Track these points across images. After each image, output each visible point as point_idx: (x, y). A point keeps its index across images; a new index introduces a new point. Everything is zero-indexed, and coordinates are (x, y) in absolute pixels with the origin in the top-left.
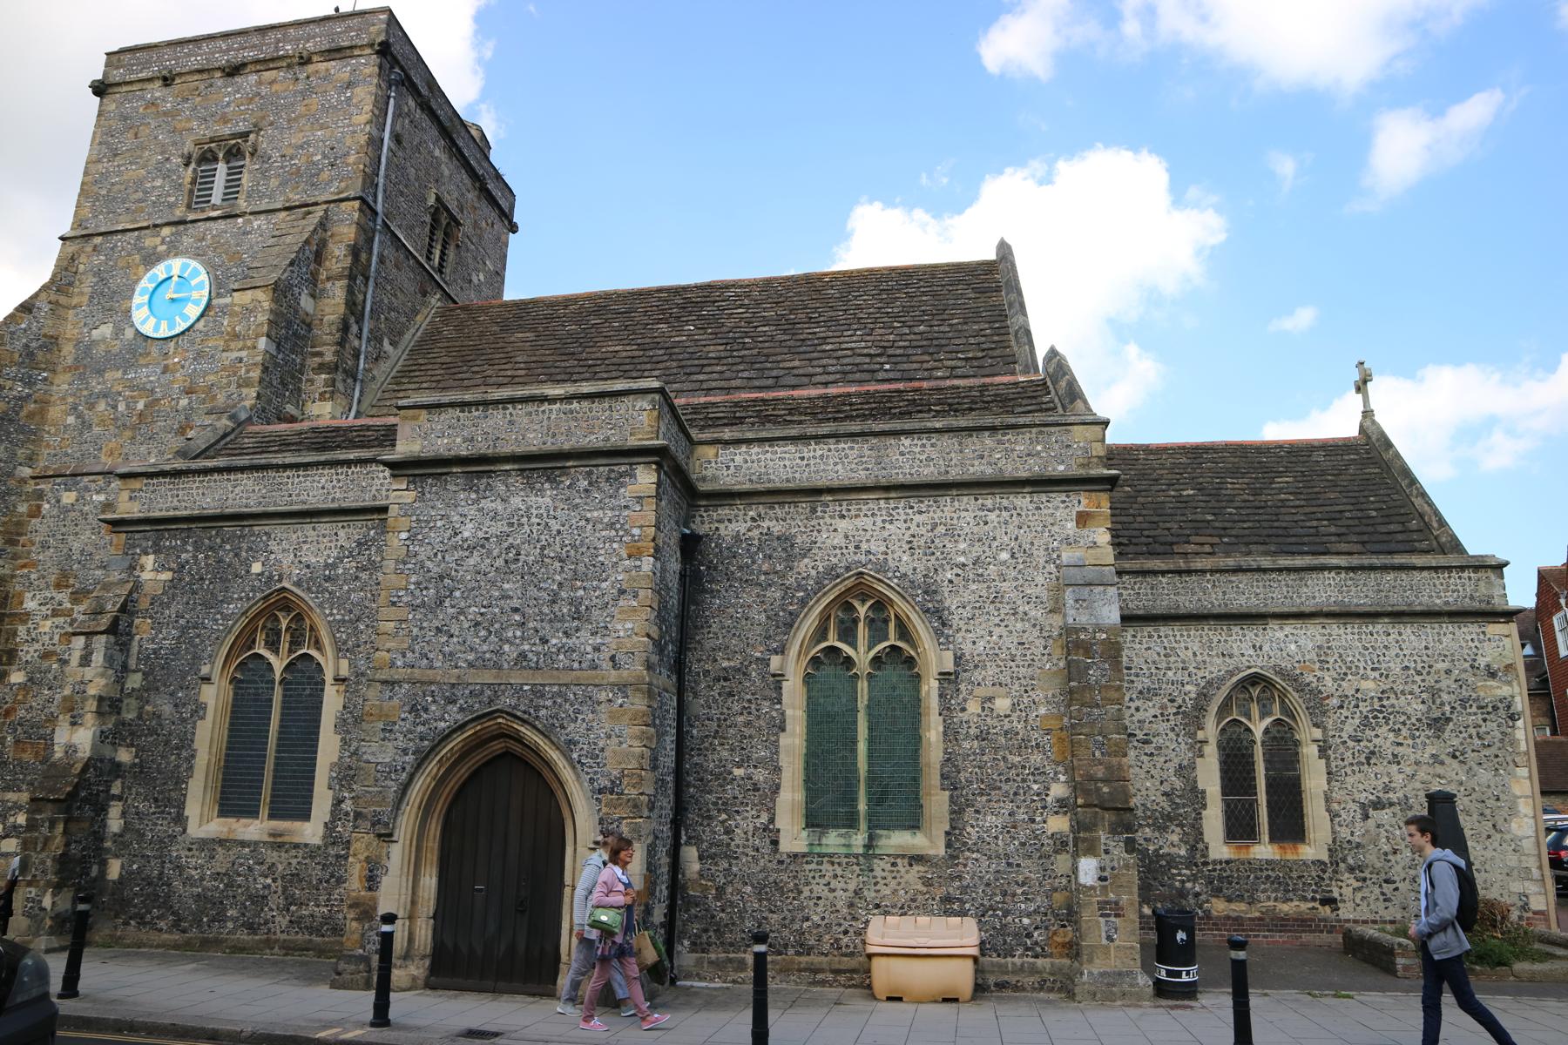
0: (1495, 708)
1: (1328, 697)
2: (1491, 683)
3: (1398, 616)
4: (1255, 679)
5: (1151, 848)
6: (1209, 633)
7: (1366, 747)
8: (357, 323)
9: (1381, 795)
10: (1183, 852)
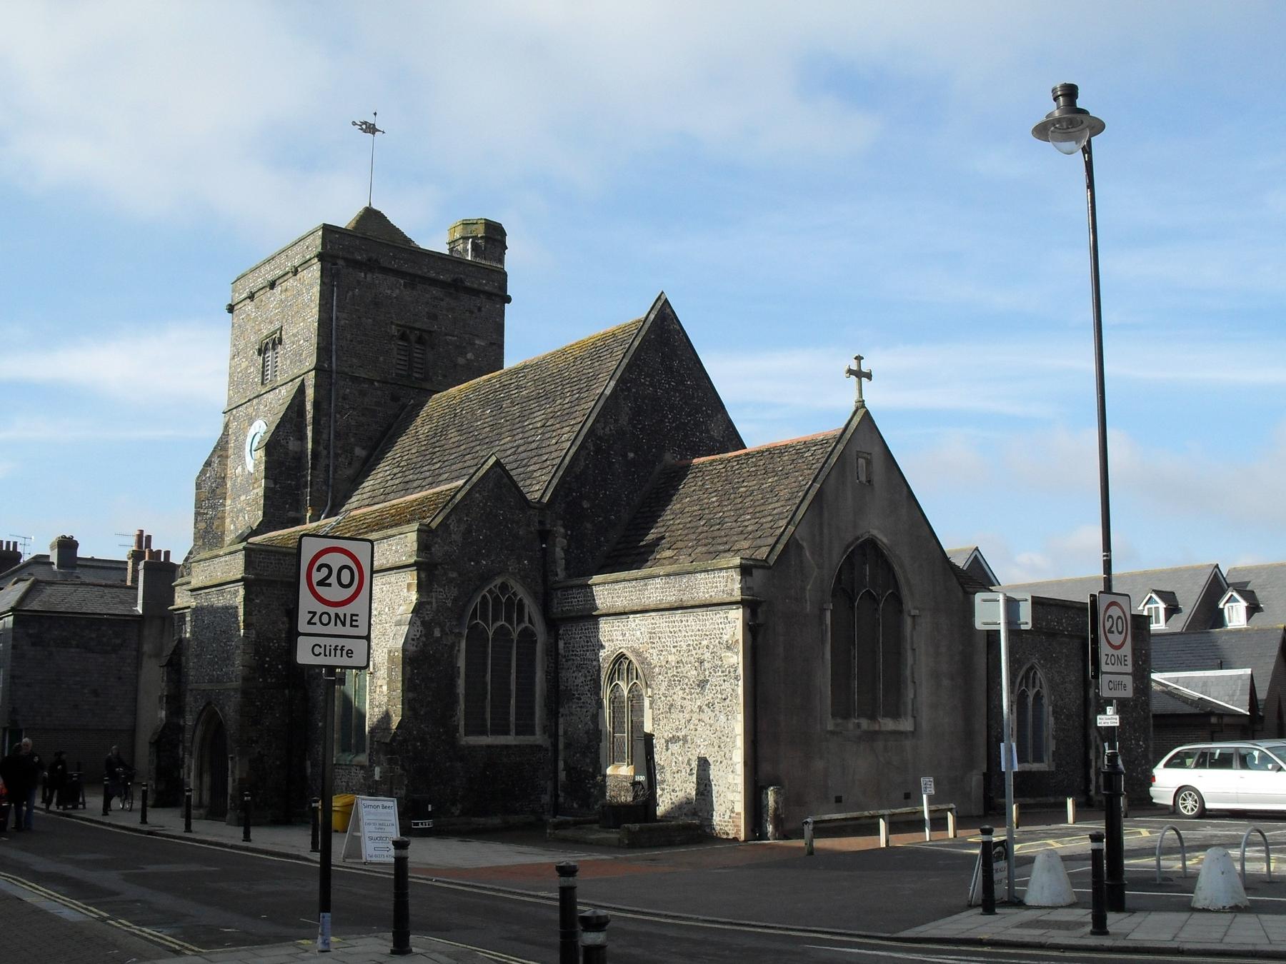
1: (655, 666)
2: (729, 654)
4: (622, 656)
5: (579, 766)
7: (669, 701)
8: (326, 449)
9: (674, 733)
10: (591, 770)
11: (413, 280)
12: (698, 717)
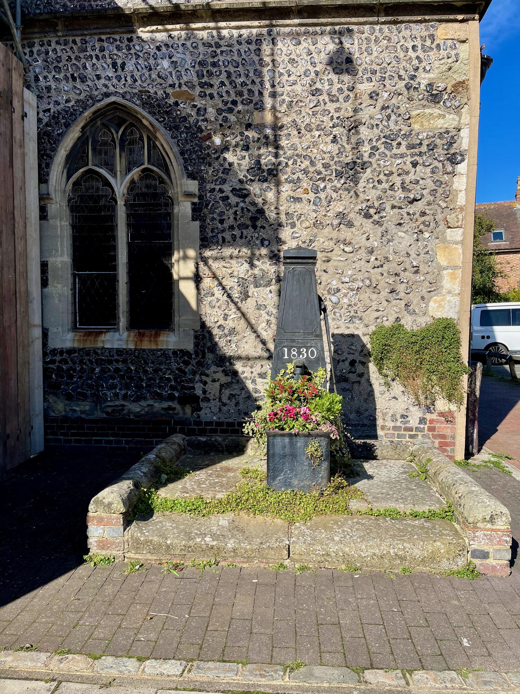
0: (432, 147)
2: (436, 111)
12: (335, 234)
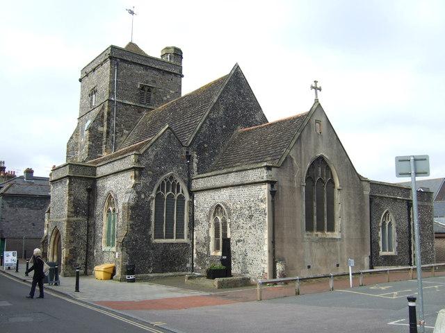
3: (243, 185)
4: (219, 206)
6: (211, 193)
11: (146, 67)
